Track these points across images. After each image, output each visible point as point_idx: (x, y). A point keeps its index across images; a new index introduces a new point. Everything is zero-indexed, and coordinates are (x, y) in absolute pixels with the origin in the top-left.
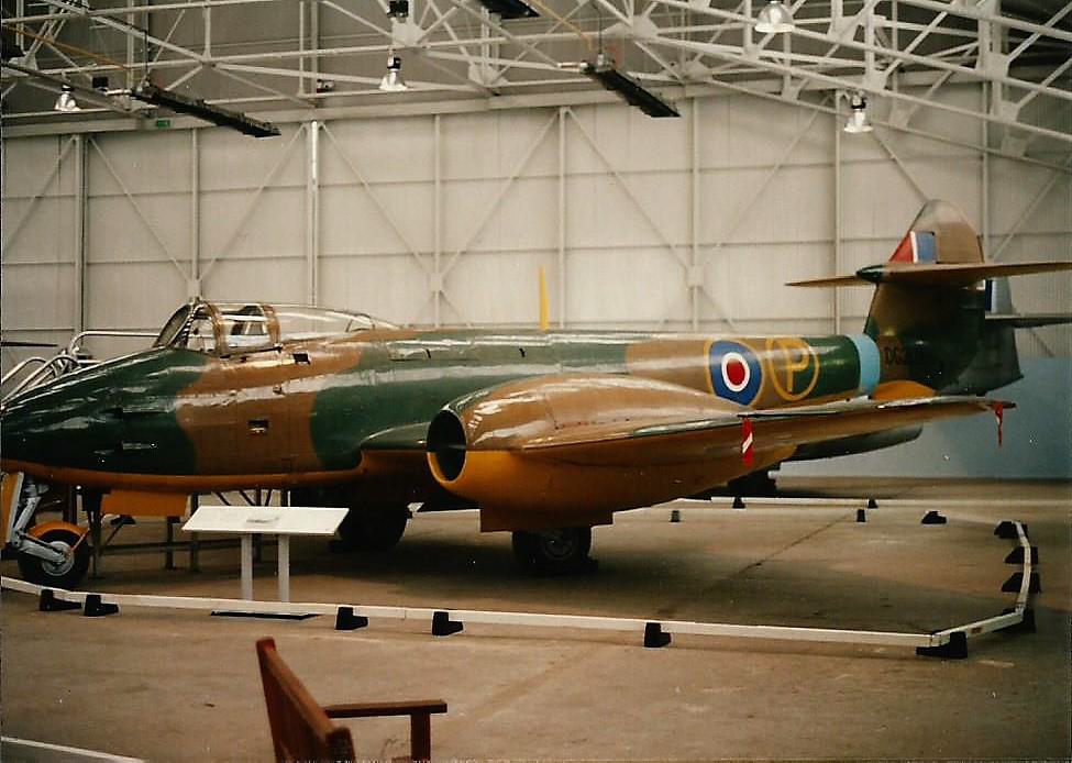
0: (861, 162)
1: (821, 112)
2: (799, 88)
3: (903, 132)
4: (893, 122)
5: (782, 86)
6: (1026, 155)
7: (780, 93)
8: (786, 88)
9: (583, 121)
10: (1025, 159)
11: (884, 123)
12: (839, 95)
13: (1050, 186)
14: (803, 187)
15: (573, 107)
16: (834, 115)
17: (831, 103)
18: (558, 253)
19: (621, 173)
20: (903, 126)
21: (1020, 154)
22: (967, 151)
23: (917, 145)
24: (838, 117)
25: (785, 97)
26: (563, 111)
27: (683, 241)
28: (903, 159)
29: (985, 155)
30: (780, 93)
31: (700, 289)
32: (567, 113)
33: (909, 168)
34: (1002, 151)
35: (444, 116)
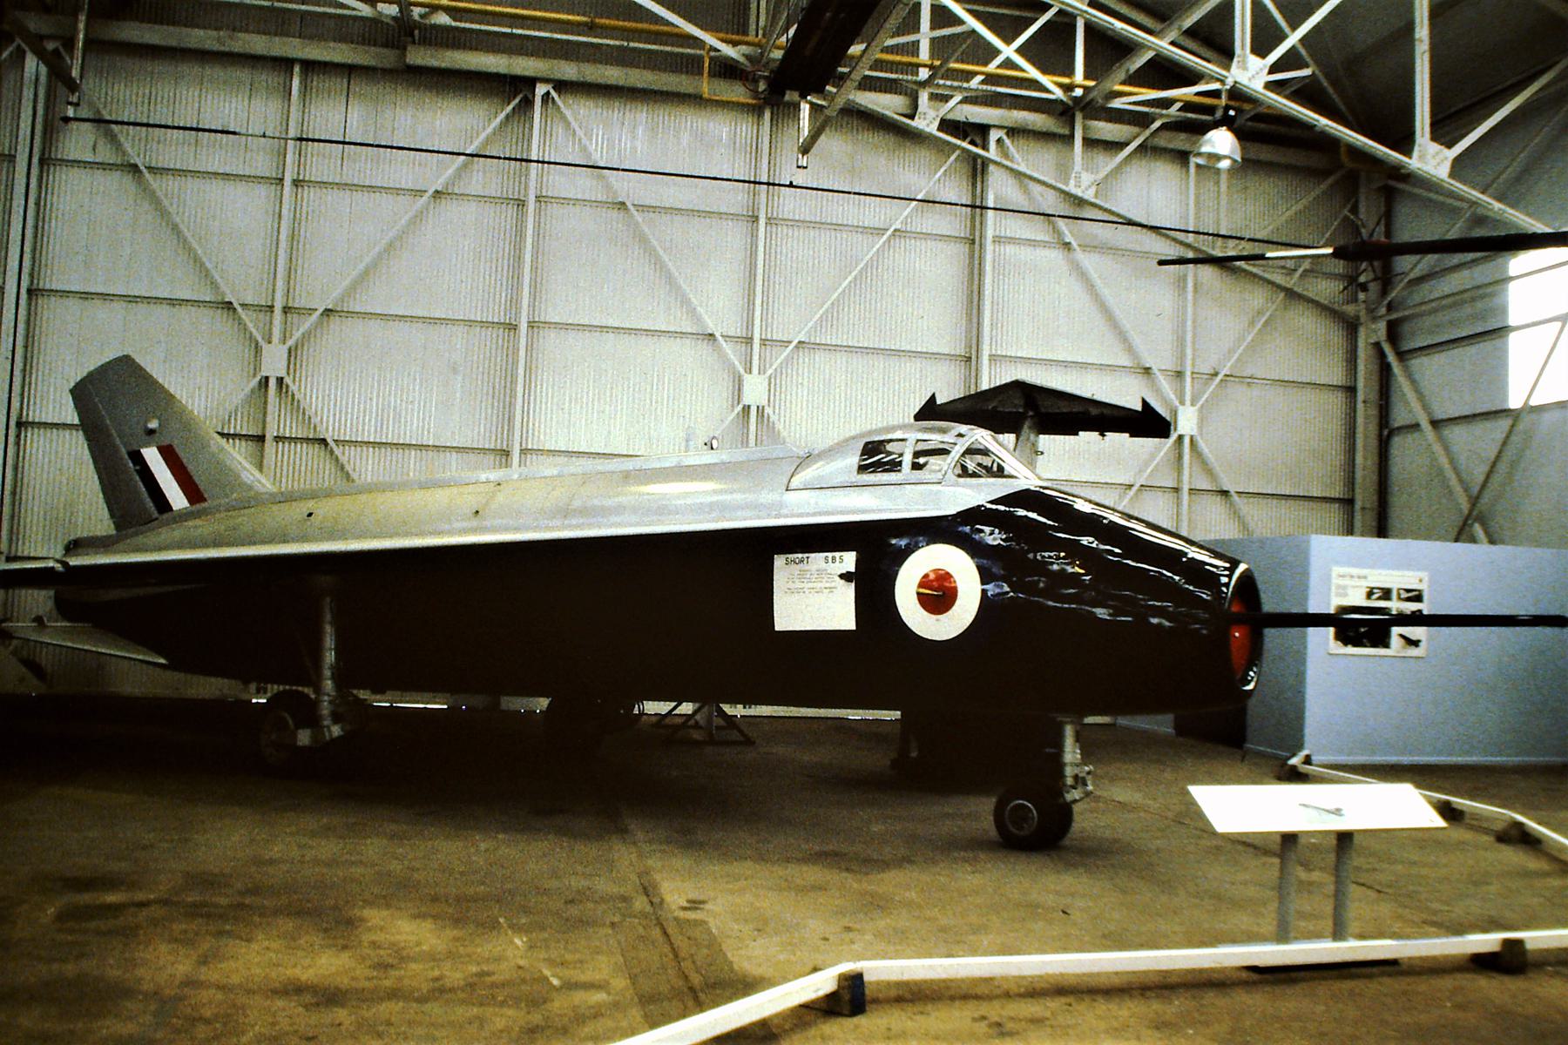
0: (1012, 240)
2: (942, 113)
3: (1080, 202)
4: (1072, 188)
7: (912, 117)
11: (1060, 185)
14: (933, 266)
15: (562, 86)
16: (986, 163)
18: (512, 332)
19: (641, 208)
20: (1089, 195)
24: (992, 168)
25: (918, 123)
26: (541, 89)
27: (736, 329)
28: (1084, 247)
31: (761, 411)
33: (1089, 261)
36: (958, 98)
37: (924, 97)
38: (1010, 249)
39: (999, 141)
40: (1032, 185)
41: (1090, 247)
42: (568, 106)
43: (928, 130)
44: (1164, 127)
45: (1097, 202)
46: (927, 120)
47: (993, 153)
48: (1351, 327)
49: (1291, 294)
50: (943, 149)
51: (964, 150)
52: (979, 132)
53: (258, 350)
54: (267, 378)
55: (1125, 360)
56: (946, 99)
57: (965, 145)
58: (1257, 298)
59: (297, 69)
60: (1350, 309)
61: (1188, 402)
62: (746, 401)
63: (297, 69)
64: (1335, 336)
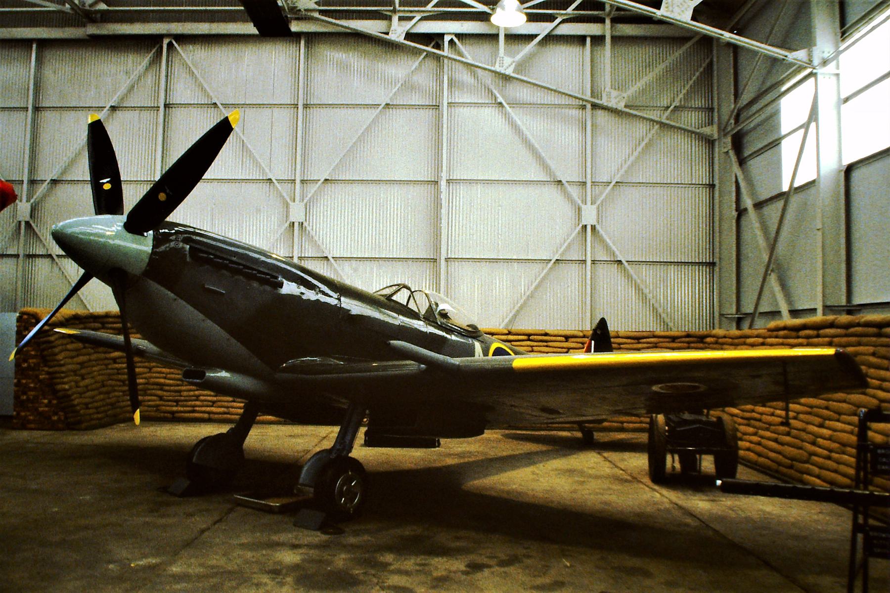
0: (464, 104)
1: (429, 55)
3: (506, 78)
4: (497, 68)
5: (390, 26)
6: (626, 106)
7: (387, 34)
8: (392, 28)
9: (189, 54)
10: (627, 110)
11: (493, 68)
12: (447, 38)
13: (646, 140)
16: (438, 58)
17: (438, 46)
20: (509, 72)
21: (621, 106)
22: (564, 101)
23: (524, 94)
25: (392, 37)
26: (166, 42)
29: (589, 106)
30: (387, 34)
32: (170, 45)
33: (516, 115)
34: (604, 102)
35: (44, 44)
36: (418, 17)
37: (395, 19)
38: (461, 110)
39: (451, 42)
40: (479, 71)
41: (514, 104)
42: (184, 51)
43: (397, 40)
44: (563, 22)
45: (516, 76)
46: (397, 31)
47: (446, 51)
48: (710, 143)
49: (662, 125)
50: (416, 52)
51: (428, 52)
52: (435, 39)
53: (287, 206)
54: (20, 222)
55: (542, 177)
56: (410, 19)
57: (429, 49)
58: (640, 129)
59: (34, 46)
60: (707, 130)
61: (589, 202)
62: (292, 219)
63: (34, 46)
64: (697, 150)
